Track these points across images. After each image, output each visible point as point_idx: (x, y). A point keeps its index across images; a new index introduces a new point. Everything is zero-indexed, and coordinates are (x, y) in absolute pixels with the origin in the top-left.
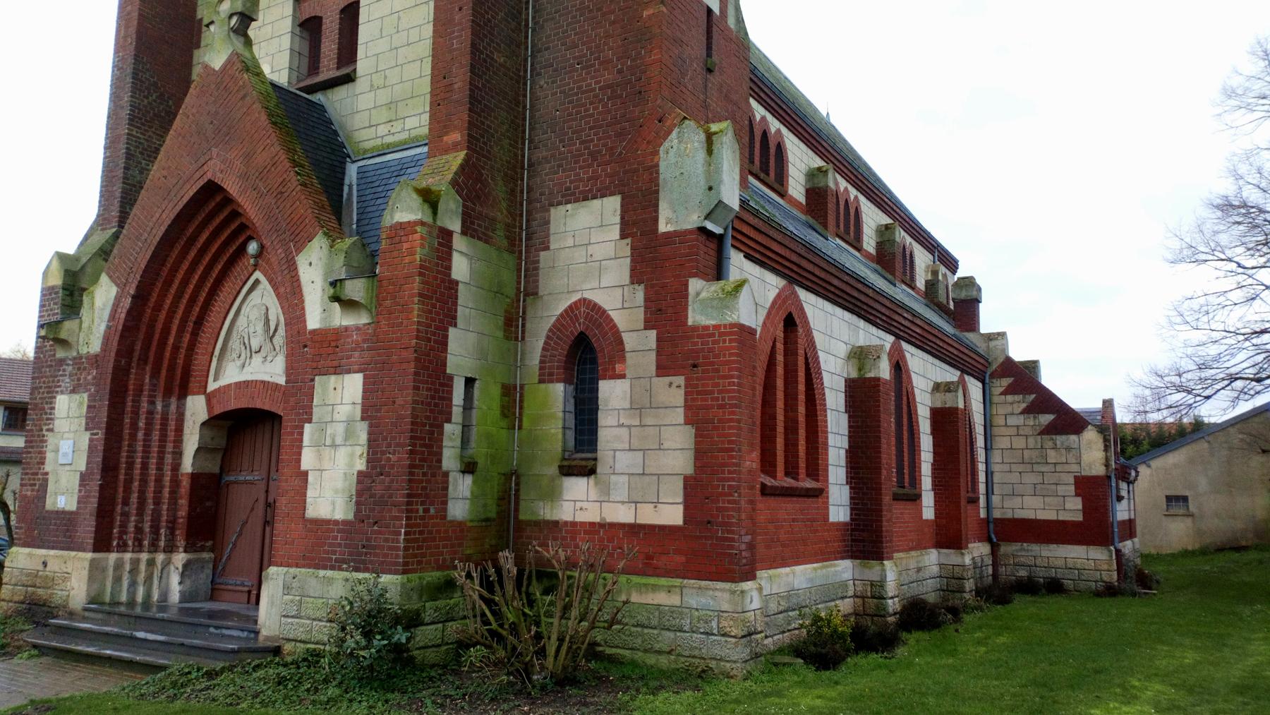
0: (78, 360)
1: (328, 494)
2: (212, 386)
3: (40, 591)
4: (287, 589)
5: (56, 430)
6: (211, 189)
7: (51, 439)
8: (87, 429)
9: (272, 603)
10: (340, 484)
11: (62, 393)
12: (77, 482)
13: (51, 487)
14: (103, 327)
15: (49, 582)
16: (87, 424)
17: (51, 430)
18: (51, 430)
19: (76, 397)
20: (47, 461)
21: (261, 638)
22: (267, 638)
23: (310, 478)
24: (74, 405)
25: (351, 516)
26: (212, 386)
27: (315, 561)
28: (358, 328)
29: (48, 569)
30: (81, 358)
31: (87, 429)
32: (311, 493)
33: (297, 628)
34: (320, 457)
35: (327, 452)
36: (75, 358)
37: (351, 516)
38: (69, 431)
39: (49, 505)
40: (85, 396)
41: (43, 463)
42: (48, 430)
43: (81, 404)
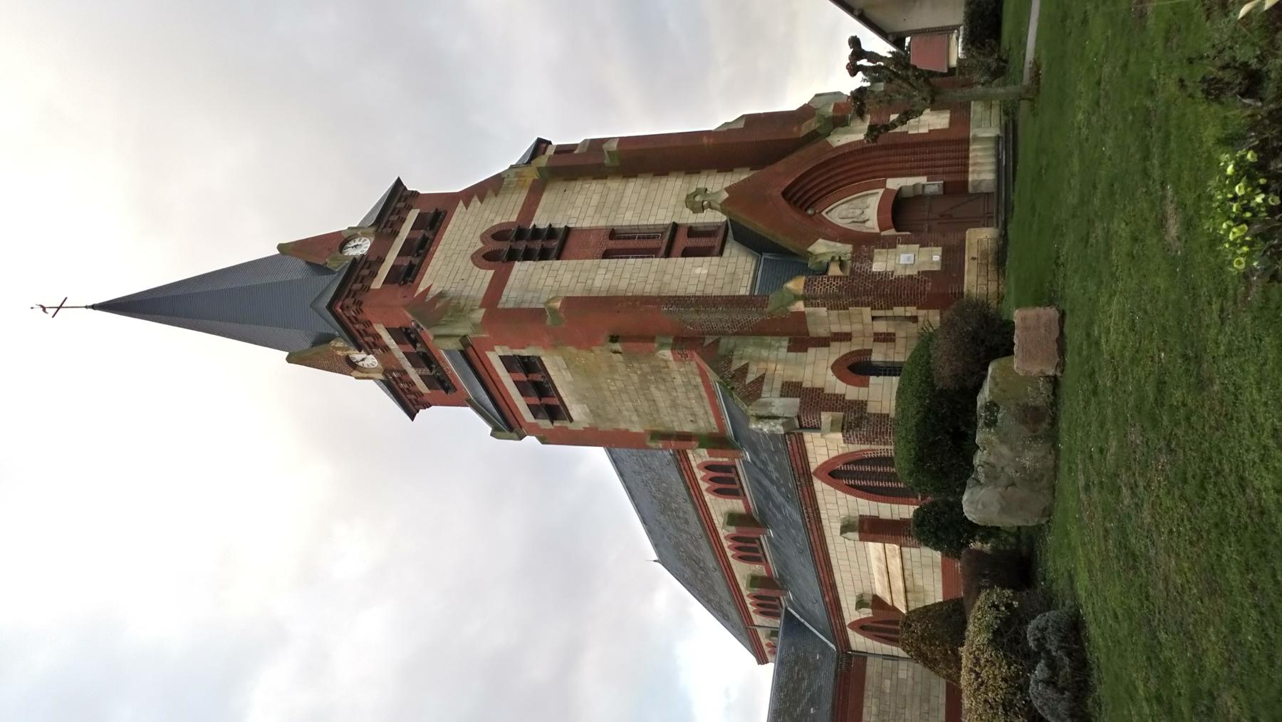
0: (853, 259)
1: (939, 120)
2: (877, 230)
3: (990, 259)
4: (979, 127)
5: (892, 269)
6: (784, 194)
7: (900, 272)
8: (895, 247)
9: (985, 132)
10: (935, 117)
11: (871, 268)
12: (925, 248)
13: (927, 268)
14: (839, 245)
15: (984, 254)
16: (892, 248)
17: (893, 272)
18: (893, 272)
19: (876, 257)
20: (911, 273)
21: (1001, 135)
22: (1001, 131)
23: (932, 128)
24: (880, 253)
25: (949, 111)
26: (877, 230)
27: (966, 122)
28: (871, 119)
29: (976, 256)
30: (853, 257)
31: (895, 247)
32: (938, 127)
33: (995, 120)
34: (924, 126)
35: (921, 123)
36: (853, 261)
37: (949, 111)
38: (895, 259)
39: (937, 268)
40: (876, 251)
41: (912, 276)
42: (892, 276)
43: (879, 252)
